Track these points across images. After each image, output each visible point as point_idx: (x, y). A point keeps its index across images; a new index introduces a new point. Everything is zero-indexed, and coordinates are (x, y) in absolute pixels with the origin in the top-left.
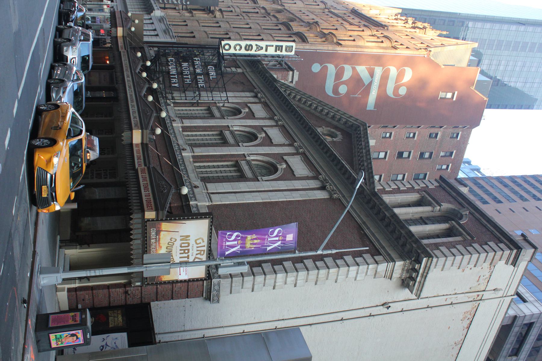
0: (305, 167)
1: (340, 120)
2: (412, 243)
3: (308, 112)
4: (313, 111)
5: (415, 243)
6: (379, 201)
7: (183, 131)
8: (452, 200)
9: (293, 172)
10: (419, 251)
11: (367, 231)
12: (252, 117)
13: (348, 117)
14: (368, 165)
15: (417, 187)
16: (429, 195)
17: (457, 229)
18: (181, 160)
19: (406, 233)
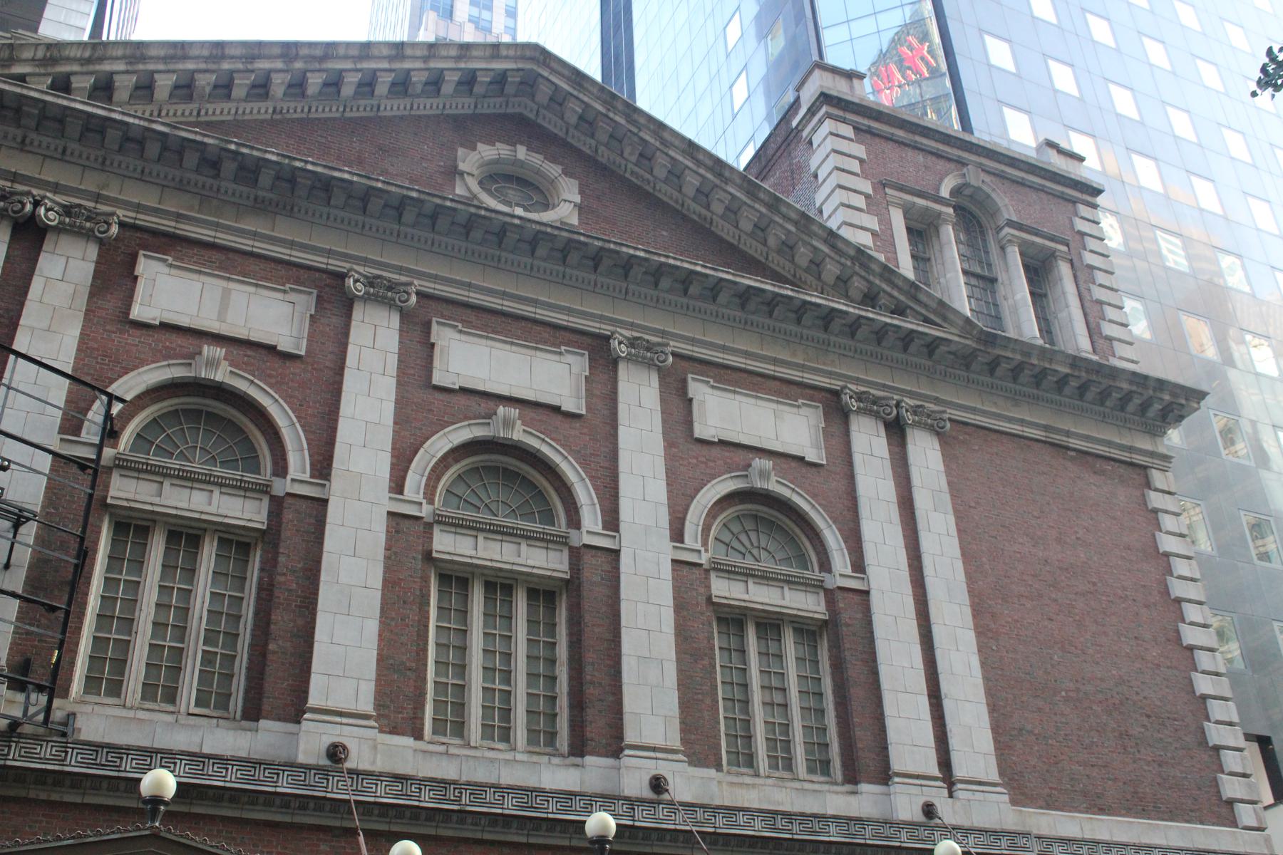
0: (760, 402)
1: (435, 83)
2: (1159, 395)
3: (275, 126)
4: (295, 109)
5: (1162, 390)
6: (1014, 351)
7: (418, 735)
8: (920, 158)
9: (802, 459)
10: (1183, 402)
11: (1074, 443)
12: (294, 368)
13: (458, 58)
14: (833, 247)
15: (867, 187)
16: (902, 189)
17: (1033, 243)
18: (780, 823)
19: (1131, 383)
